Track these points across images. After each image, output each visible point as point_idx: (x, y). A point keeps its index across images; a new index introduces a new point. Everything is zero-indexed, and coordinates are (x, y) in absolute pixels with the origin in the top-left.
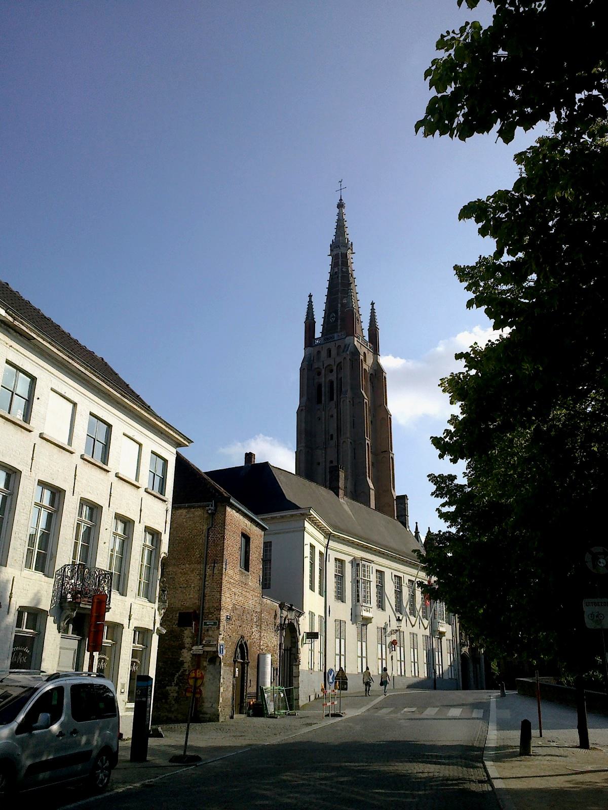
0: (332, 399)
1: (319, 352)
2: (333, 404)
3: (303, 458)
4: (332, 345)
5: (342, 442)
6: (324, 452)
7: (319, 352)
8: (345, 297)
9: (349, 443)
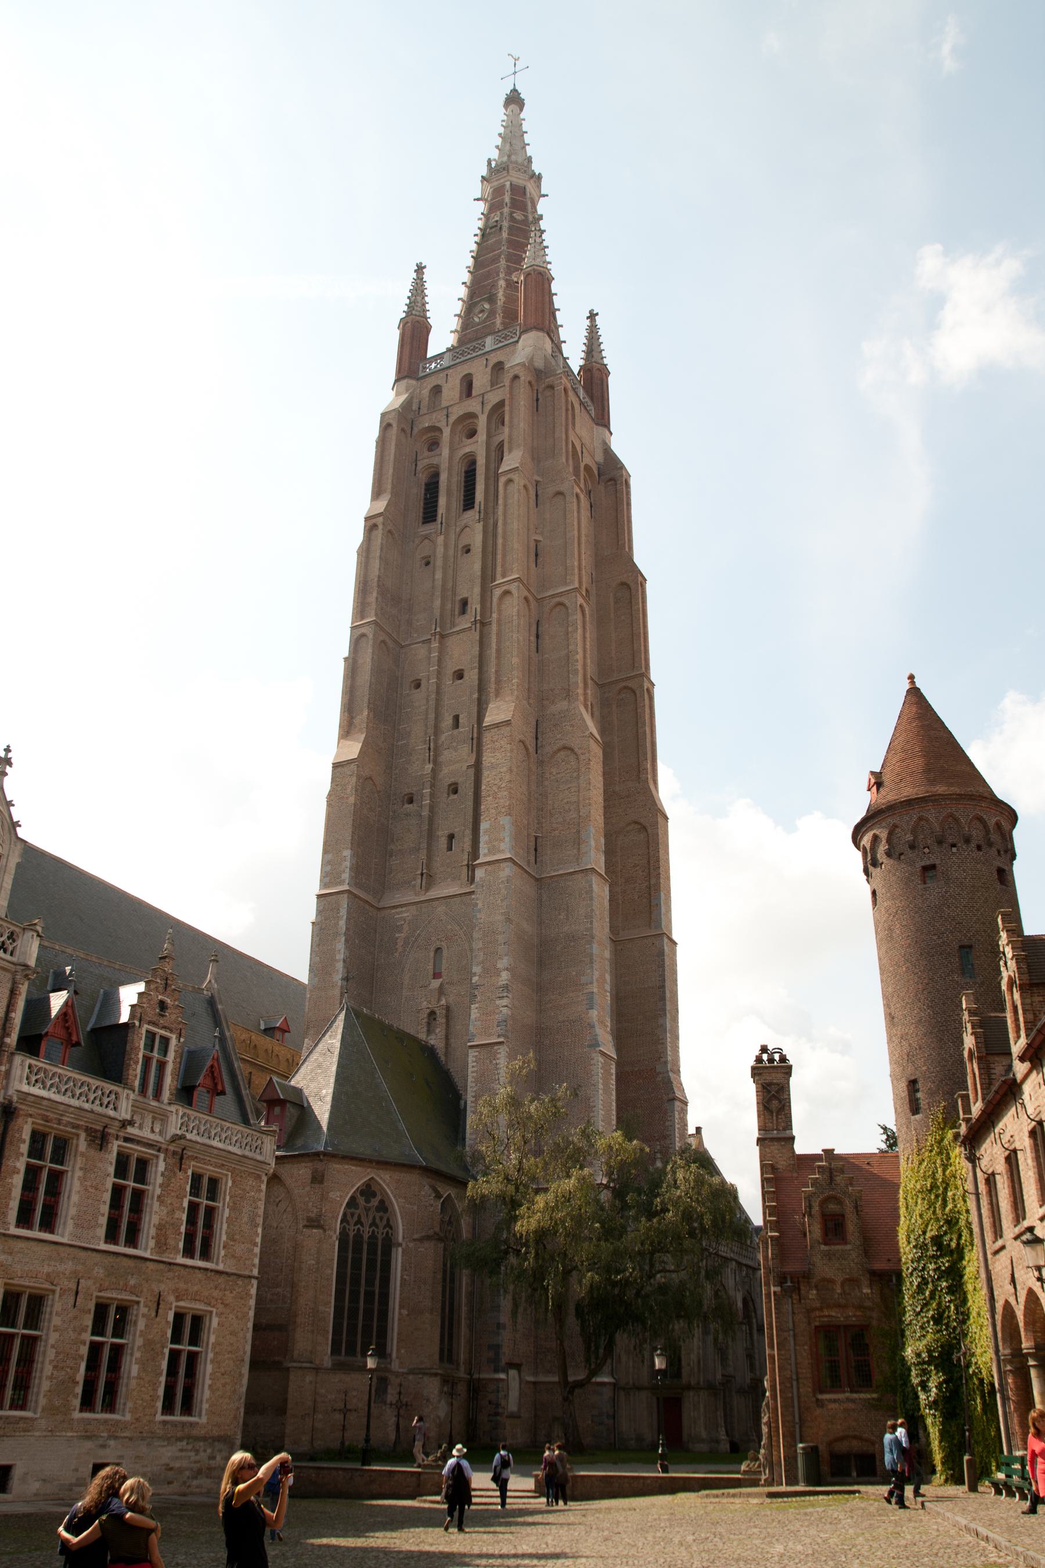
0: (469, 503)
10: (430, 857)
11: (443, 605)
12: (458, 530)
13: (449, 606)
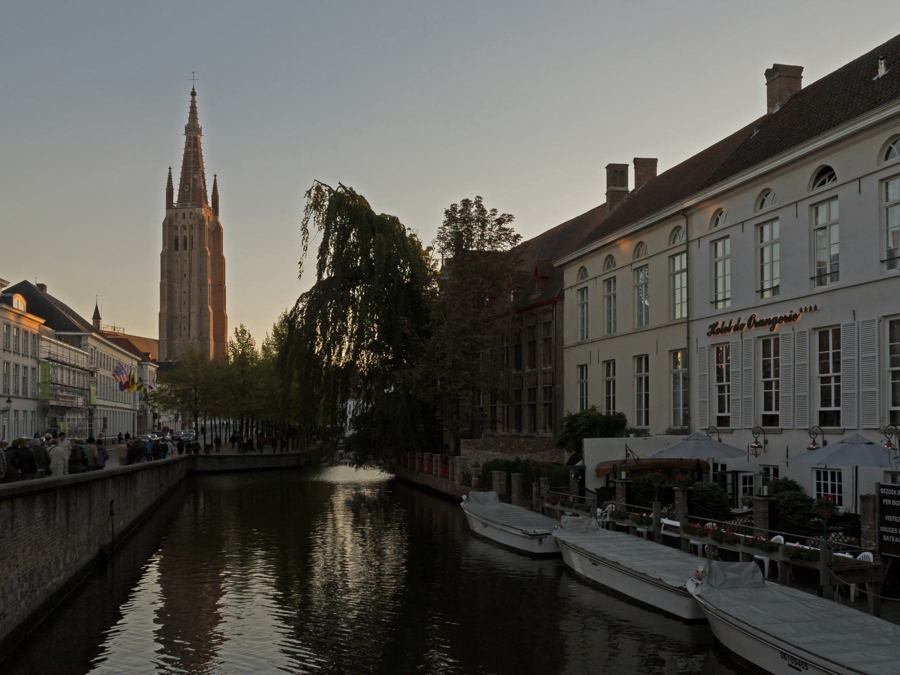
0: (185, 249)
1: (176, 214)
2: (186, 252)
3: (166, 288)
4: (186, 211)
7: (176, 214)
8: (196, 173)
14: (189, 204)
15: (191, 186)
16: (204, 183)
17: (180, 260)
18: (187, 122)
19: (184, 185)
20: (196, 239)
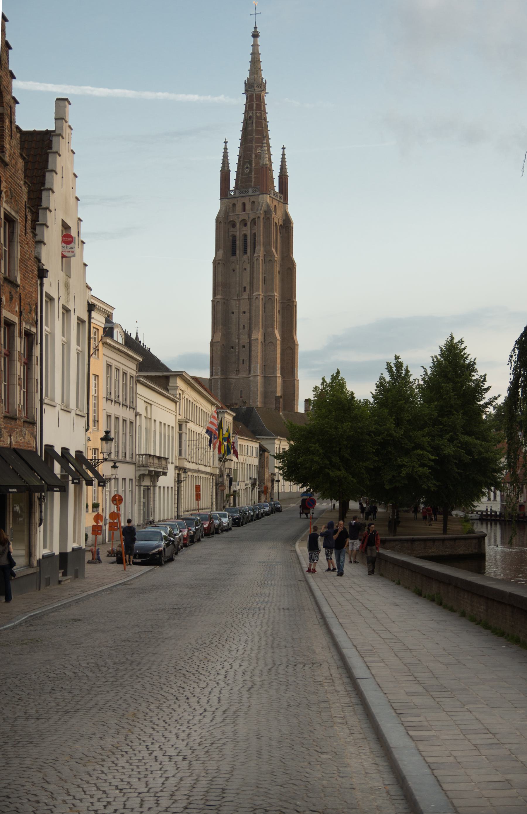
0: (245, 252)
1: (234, 205)
2: (245, 257)
3: (220, 308)
4: (247, 201)
5: (255, 297)
6: (237, 303)
8: (259, 146)
9: (261, 298)
10: (238, 366)
11: (239, 289)
12: (243, 262)
13: (241, 289)
14: (250, 190)
15: (254, 165)
16: (270, 159)
17: (238, 270)
18: (246, 75)
19: (244, 163)
20: (261, 238)
